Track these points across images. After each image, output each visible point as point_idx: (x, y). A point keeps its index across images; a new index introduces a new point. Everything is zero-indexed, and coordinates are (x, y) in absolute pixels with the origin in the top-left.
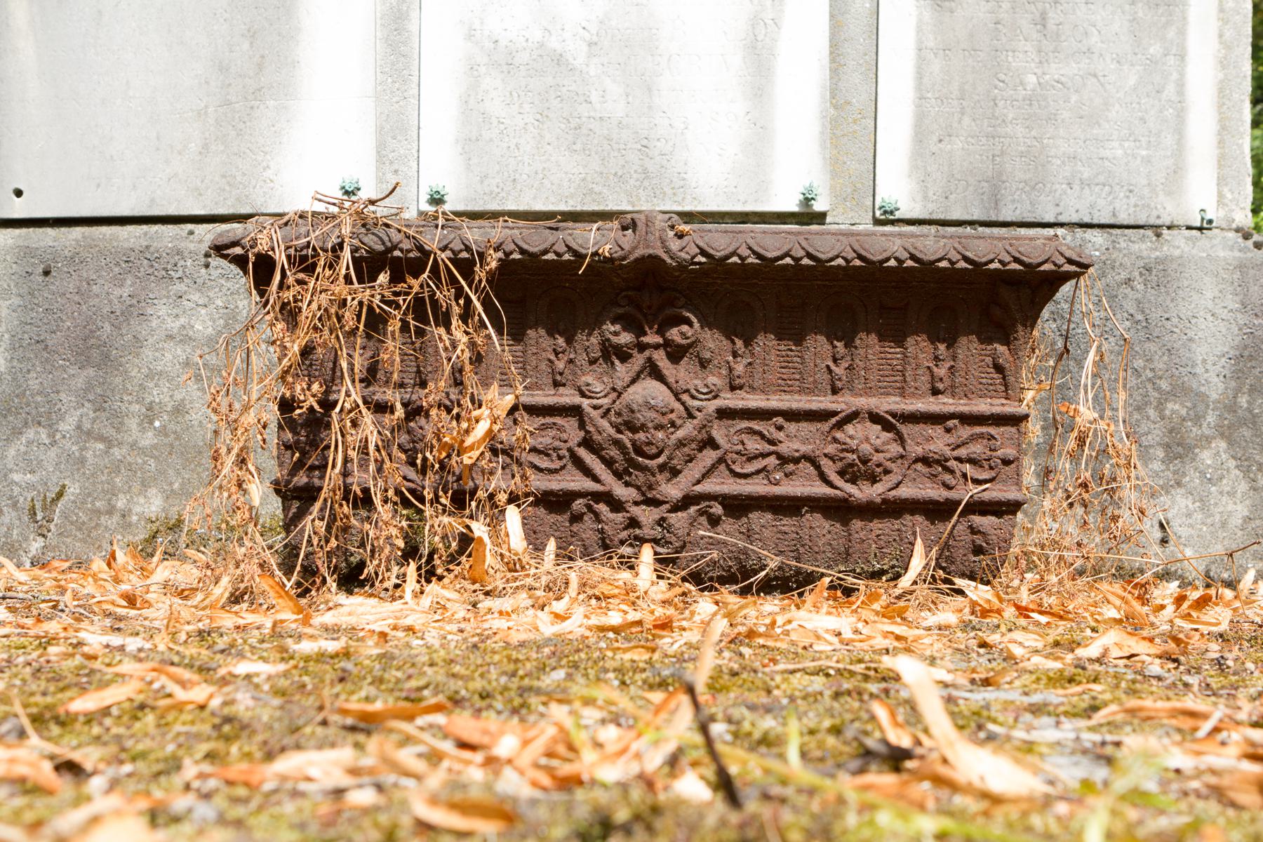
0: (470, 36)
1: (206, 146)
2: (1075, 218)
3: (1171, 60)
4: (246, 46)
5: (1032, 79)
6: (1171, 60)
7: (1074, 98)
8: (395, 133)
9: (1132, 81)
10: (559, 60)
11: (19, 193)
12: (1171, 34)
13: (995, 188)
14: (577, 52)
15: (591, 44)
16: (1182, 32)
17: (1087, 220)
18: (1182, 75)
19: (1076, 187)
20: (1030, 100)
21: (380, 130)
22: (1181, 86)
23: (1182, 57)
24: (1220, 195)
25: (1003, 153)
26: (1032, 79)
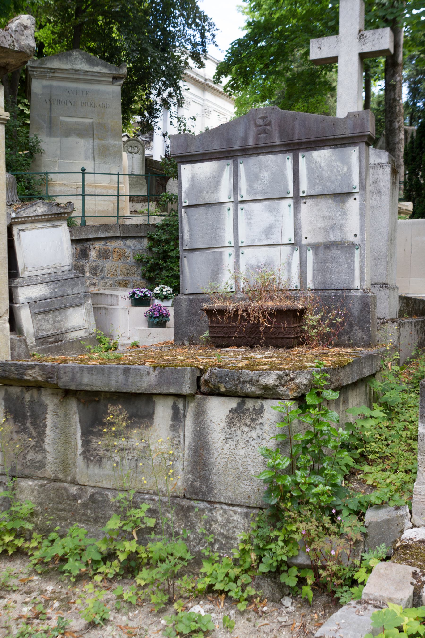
13: (325, 283)
22: (354, 267)
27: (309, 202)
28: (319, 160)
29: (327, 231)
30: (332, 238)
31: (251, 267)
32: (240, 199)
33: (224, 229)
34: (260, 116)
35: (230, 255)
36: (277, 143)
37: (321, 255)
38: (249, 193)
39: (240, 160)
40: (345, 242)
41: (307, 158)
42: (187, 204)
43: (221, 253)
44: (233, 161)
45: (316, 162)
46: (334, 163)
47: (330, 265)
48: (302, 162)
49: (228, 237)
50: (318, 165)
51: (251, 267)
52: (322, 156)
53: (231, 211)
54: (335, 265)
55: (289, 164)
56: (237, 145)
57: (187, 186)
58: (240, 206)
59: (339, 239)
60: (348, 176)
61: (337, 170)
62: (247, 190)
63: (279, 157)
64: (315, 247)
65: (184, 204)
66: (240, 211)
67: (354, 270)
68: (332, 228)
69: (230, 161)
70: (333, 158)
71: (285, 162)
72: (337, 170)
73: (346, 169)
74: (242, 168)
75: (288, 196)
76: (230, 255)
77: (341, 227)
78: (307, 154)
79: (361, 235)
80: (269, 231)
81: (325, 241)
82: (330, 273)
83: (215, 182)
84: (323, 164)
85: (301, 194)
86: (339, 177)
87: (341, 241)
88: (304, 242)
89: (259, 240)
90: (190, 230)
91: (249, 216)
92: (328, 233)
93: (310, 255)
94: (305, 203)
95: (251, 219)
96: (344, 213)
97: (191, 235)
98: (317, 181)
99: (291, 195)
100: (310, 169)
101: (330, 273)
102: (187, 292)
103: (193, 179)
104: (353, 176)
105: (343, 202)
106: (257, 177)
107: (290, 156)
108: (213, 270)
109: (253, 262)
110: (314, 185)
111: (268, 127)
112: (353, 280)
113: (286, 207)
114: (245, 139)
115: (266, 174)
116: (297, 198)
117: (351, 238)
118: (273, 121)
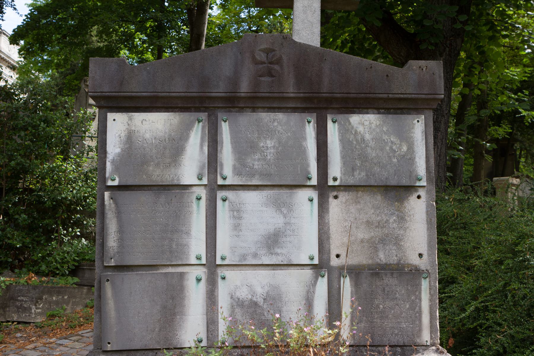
0: (232, 298)
1: (160, 330)
2: (393, 344)
3: (417, 300)
4: (171, 301)
5: (381, 306)
6: (417, 300)
7: (393, 311)
8: (211, 323)
9: (408, 306)
10: (256, 304)
11: (109, 343)
12: (417, 293)
14: (260, 301)
15: (264, 299)
16: (420, 293)
17: (397, 344)
18: (420, 304)
19: (394, 335)
20: (381, 312)
21: (207, 322)
22: (420, 307)
23: (420, 300)
24: (431, 336)
25: (374, 327)
26: (381, 306)
27: (343, 196)
28: (361, 129)
29: (373, 245)
30: (382, 257)
31: (238, 304)
32: (220, 182)
33: (188, 233)
34: (263, 46)
35: (199, 280)
36: (292, 95)
37: (365, 286)
38: (237, 172)
39: (221, 115)
40: (403, 266)
41: (340, 124)
42: (116, 183)
43: (182, 275)
44: (209, 116)
45: (356, 132)
46: (385, 137)
47: (381, 304)
48: (333, 130)
49: (197, 246)
50: (359, 138)
51: (238, 304)
52: (367, 123)
53: (203, 203)
54: (389, 304)
55: (310, 131)
56: (220, 89)
57: (118, 150)
58: (220, 194)
59: (394, 260)
60: (409, 159)
61: (391, 148)
62: (235, 168)
63: (294, 118)
64: (355, 272)
65: (110, 183)
66: (219, 203)
67: (420, 312)
68: (383, 241)
69: (203, 116)
70: (385, 129)
71: (304, 126)
72: (391, 148)
73: (405, 148)
74: (225, 128)
75: (309, 183)
76: (199, 280)
77: (397, 241)
78: (340, 117)
79: (429, 255)
80: (273, 240)
81: (370, 262)
82: (382, 318)
83: (175, 148)
84: (368, 137)
85: (331, 183)
86: (395, 160)
87: (398, 264)
88: (335, 262)
89: (255, 255)
90: (121, 230)
91: (237, 213)
92: (376, 250)
93: (347, 285)
94: (336, 197)
95: (240, 218)
96: (402, 219)
97: (121, 240)
98: (358, 163)
99: (314, 182)
100: (343, 141)
101: (382, 318)
102: (109, 347)
103: (130, 138)
104: (417, 159)
105: (401, 200)
106: (253, 147)
107: (312, 118)
108: (165, 307)
109: (243, 294)
110: (353, 170)
111: (276, 67)
112: (420, 330)
113: (305, 202)
114: (235, 81)
115: (270, 143)
116: (324, 189)
117: (414, 260)
118: (285, 58)
